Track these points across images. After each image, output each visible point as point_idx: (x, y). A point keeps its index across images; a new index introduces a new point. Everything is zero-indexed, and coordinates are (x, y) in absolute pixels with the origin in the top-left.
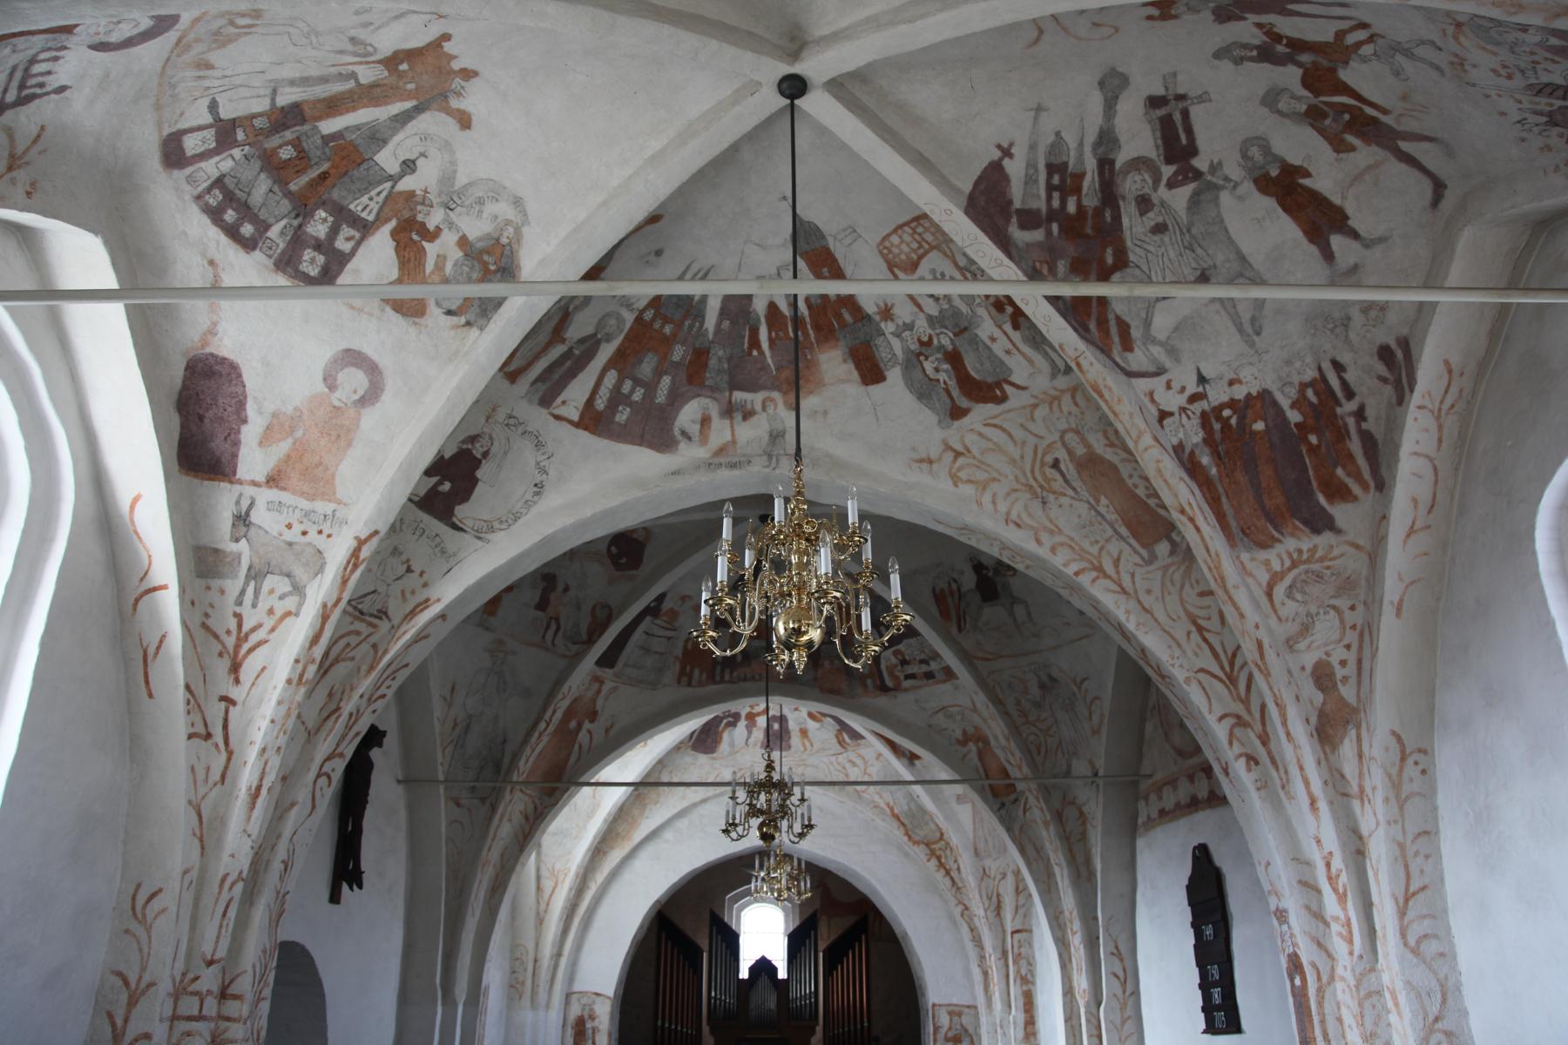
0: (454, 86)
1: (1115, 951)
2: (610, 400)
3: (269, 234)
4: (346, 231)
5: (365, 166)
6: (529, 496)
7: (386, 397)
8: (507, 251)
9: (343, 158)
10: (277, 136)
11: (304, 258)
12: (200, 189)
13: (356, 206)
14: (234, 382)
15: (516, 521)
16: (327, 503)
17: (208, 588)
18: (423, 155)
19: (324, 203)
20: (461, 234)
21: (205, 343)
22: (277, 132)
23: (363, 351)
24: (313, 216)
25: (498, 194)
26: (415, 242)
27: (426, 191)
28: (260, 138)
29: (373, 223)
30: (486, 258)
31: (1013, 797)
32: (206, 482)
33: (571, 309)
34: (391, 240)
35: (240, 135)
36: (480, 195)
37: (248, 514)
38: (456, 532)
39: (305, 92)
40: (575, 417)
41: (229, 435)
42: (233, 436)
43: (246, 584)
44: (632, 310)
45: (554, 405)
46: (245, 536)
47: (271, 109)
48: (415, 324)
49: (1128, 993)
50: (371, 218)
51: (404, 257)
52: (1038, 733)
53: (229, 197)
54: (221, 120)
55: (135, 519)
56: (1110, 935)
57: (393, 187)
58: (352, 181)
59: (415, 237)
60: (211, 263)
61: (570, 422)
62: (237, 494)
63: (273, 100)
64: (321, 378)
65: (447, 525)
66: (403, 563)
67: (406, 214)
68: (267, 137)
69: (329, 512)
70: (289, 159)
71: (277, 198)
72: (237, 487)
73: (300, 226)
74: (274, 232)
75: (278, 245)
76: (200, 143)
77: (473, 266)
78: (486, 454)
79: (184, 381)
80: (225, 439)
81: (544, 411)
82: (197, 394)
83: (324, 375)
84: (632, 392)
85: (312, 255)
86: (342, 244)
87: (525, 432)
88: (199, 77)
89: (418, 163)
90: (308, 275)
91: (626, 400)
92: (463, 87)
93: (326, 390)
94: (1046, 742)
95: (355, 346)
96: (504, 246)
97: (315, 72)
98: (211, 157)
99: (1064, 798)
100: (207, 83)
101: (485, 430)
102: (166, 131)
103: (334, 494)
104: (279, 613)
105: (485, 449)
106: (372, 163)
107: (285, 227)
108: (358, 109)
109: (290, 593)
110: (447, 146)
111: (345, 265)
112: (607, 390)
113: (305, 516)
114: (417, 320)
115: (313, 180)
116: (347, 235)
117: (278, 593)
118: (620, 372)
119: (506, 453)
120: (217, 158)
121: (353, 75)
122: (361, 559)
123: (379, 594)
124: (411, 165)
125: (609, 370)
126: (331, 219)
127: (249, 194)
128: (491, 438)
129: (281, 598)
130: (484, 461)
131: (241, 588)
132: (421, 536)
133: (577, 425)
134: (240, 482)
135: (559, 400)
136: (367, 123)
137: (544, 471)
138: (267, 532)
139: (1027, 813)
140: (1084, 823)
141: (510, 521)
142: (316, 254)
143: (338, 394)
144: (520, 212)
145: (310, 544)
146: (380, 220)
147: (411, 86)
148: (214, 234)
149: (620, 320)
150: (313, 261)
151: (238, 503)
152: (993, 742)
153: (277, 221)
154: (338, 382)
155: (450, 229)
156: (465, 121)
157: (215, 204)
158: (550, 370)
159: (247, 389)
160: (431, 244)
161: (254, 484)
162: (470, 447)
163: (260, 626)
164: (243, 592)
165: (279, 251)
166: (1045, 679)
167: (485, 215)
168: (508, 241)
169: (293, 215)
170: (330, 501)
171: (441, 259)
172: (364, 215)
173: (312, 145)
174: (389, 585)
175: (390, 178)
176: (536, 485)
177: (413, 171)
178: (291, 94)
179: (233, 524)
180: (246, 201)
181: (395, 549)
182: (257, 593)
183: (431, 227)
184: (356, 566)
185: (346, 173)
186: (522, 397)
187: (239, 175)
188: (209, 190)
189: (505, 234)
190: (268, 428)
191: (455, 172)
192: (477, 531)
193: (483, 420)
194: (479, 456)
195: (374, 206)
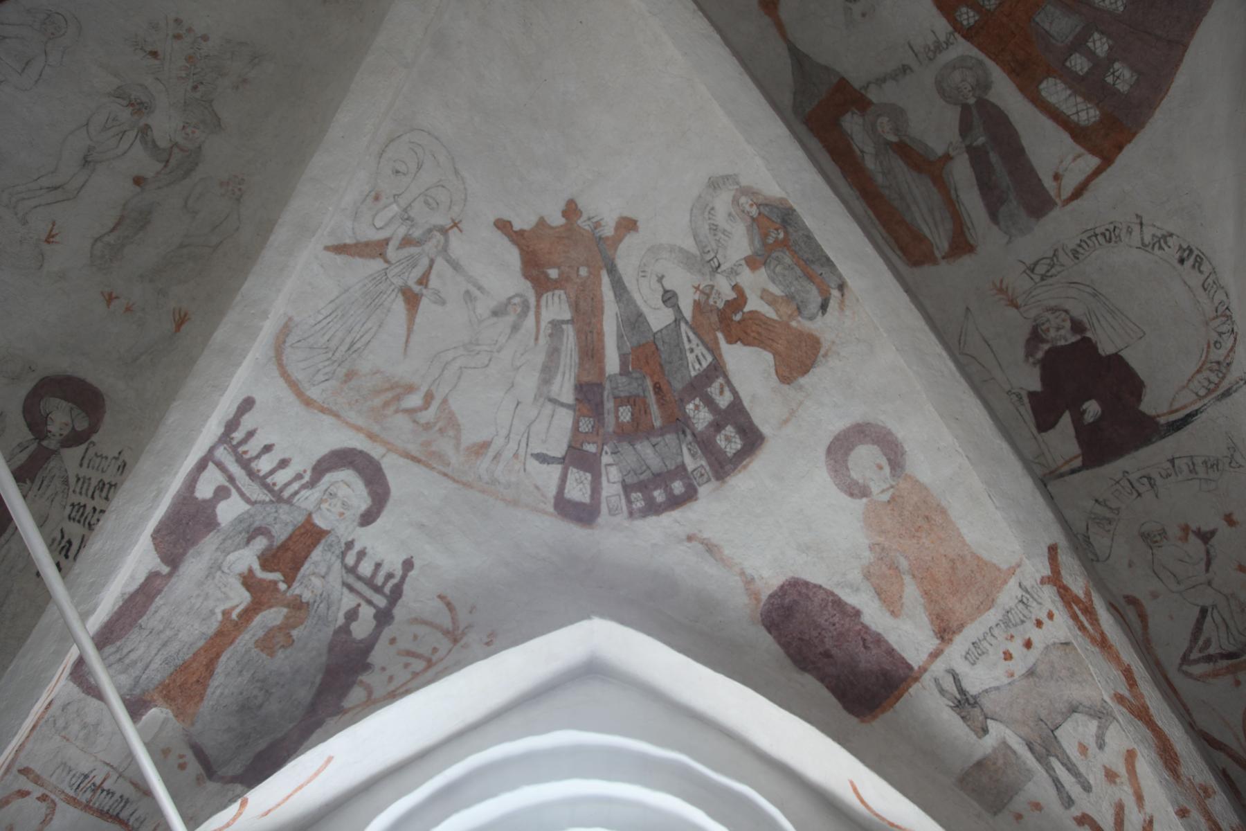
0: (587, 228)
2: (1087, 98)
3: (690, 467)
4: (713, 390)
5: (660, 344)
6: (1195, 280)
7: (900, 432)
8: (766, 211)
9: (647, 363)
10: (606, 415)
11: (723, 446)
12: (625, 508)
13: (694, 369)
14: (811, 594)
15: (1229, 317)
16: (1007, 587)
17: (1019, 817)
18: (660, 279)
19: (682, 400)
20: (743, 262)
21: (755, 595)
22: (603, 414)
23: (837, 432)
24: (689, 418)
25: (707, 205)
26: (743, 320)
27: (697, 288)
28: (601, 431)
29: (715, 358)
30: (771, 240)
32: (898, 705)
33: (893, 139)
34: (735, 346)
35: (591, 448)
36: (707, 227)
37: (962, 691)
38: (1190, 427)
39: (564, 374)
40: (1093, 162)
41: (864, 640)
42: (867, 637)
43: (1049, 769)
44: (948, 43)
45: (1053, 193)
46: (986, 718)
47: (574, 411)
48: (825, 355)
50: (710, 359)
51: (755, 338)
53: (643, 487)
54: (564, 458)
55: (878, 811)
57: (687, 323)
58: (670, 363)
59: (738, 317)
60: (690, 538)
61: (1097, 172)
62: (932, 685)
63: (563, 405)
64: (849, 499)
65: (1163, 437)
66: (1185, 539)
67: (714, 318)
68: (603, 426)
69: (1019, 593)
70: (632, 415)
71: (662, 443)
72: (927, 677)
73: (694, 435)
74: (690, 464)
75: (702, 466)
76: (581, 486)
77: (777, 259)
78: (1077, 327)
79: (779, 643)
80: (866, 647)
81: (1055, 213)
82: (800, 639)
83: (845, 492)
84: (1091, 55)
85: (723, 437)
86: (724, 401)
87: (1075, 254)
88: (495, 458)
89: (668, 287)
90: (739, 451)
91: (1100, 66)
92: (589, 219)
93: (865, 500)
95: (827, 441)
96: (760, 214)
97: (540, 358)
98: (600, 483)
100: (508, 454)
101: (1033, 313)
102: (550, 508)
103: (999, 570)
104: (1121, 769)
105: (1068, 324)
106: (658, 336)
107: (689, 449)
108: (602, 329)
109: (1102, 730)
110: (654, 250)
111: (743, 407)
112: (1072, 99)
113: (1007, 626)
114: (822, 352)
115: (658, 401)
116: (718, 391)
117: (1091, 743)
118: (1049, 73)
119: (1095, 294)
120: (604, 479)
121: (556, 325)
122: (1081, 594)
123: (1214, 606)
124: (668, 295)
125: (1039, 92)
126: (697, 401)
127: (648, 468)
128: (1053, 310)
129: (1101, 746)
130: (1089, 334)
131: (1050, 780)
132: (1152, 486)
133: (1107, 161)
134: (923, 670)
135: (1048, 183)
136: (618, 327)
137: (1162, 240)
138: (997, 688)
141: (1225, 328)
142: (723, 432)
143: (875, 489)
144: (724, 184)
145: (1047, 647)
146: (714, 350)
147: (583, 272)
148: (667, 519)
149: (961, 63)
150: (728, 439)
151: (942, 691)
153: (681, 454)
154: (861, 481)
155: (737, 274)
156: (628, 225)
157: (643, 503)
158: (986, 186)
159: (824, 586)
160: (749, 302)
161: (935, 655)
162: (1046, 347)
163: (1120, 810)
164: (1057, 783)
165: (708, 468)
167: (728, 228)
168: (755, 207)
169: (682, 436)
170: (1005, 582)
171: (765, 295)
172: (705, 365)
173: (626, 387)
174: (1209, 583)
175: (677, 322)
176: (1182, 261)
177: (674, 295)
178: (562, 386)
179: (963, 718)
180: (653, 474)
181: (1145, 536)
182: (1071, 768)
183: (731, 295)
184: (1089, 611)
185: (661, 365)
186: (1009, 242)
187: (629, 468)
188: (629, 502)
189: (747, 208)
190: (879, 594)
191: (681, 250)
192: (1210, 392)
193: (1012, 312)
194: (1078, 337)
195: (700, 350)
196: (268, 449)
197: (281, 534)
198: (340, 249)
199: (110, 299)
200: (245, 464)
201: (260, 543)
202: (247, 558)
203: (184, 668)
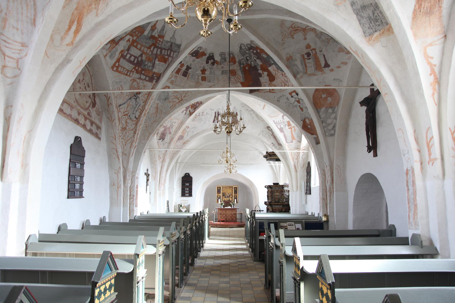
196: (279, 121)
197: (287, 124)
198: (263, 108)
199: (262, 121)
200: (279, 123)
201: (287, 126)
202: (287, 127)
203: (292, 137)
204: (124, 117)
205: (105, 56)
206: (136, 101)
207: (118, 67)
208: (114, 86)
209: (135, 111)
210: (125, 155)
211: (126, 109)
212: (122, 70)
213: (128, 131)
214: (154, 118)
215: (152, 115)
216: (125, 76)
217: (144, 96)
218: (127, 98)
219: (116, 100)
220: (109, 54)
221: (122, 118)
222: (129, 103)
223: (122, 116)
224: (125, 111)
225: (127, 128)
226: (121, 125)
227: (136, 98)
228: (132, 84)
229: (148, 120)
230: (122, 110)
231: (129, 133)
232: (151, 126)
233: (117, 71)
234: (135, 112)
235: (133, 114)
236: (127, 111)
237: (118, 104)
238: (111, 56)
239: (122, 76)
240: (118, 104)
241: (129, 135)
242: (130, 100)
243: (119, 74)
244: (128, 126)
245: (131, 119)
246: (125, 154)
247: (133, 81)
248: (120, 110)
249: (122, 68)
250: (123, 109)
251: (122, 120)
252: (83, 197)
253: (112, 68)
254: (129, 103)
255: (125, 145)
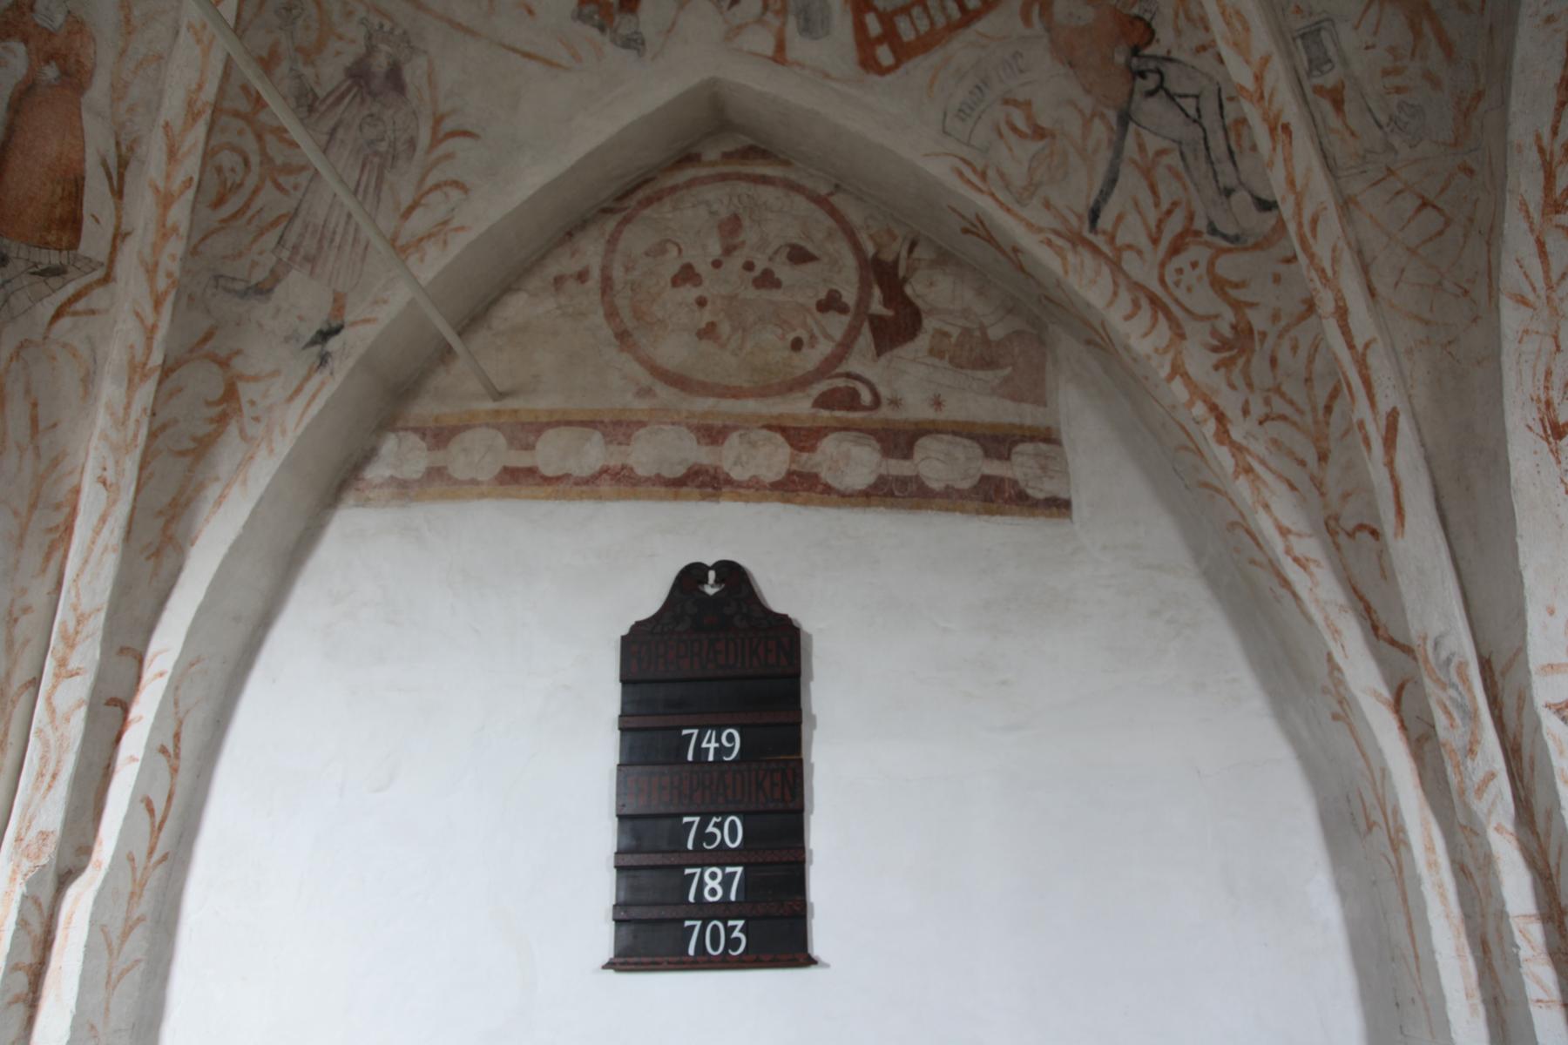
1: (171, 749)
31: (54, 258)
49: (156, 856)
52: (255, 159)
56: (176, 704)
94: (256, 191)
99: (208, 337)
139: (66, 322)
140: (222, 420)
152: (97, 93)
166: (380, 63)
204: (1181, 261)
205: (779, 54)
206: (1171, 97)
207: (890, 35)
208: (968, 144)
209: (1225, 168)
210: (1364, 537)
211: (1157, 205)
212: (923, 26)
213: (1280, 336)
214: (1436, 83)
215: (1397, 81)
216: (969, 34)
217: (1189, 19)
218: (1099, 131)
219: (1047, 205)
220: (792, 25)
221: (1169, 280)
222: (1142, 147)
223: (1162, 265)
224: (1153, 224)
225: (1258, 320)
226: (1197, 335)
227: (1151, 82)
228: (1048, 29)
229: (1396, 141)
230: (1133, 232)
231: (1295, 349)
232: (1470, 172)
233: (903, 52)
234: (1227, 177)
235: (1228, 192)
236: (1169, 212)
237: (1074, 221)
238: (807, 20)
239: (961, 50)
240: (1074, 221)
241: (1311, 360)
242: (1132, 127)
243: (936, 57)
244: (1252, 305)
245: (1235, 239)
246: (1361, 527)
247: (1036, 10)
248: (1119, 241)
249: (916, 11)
250: (1132, 219)
251: (1180, 293)
252: (810, 961)
253: (869, 63)
254: (1142, 147)
255: (1323, 457)
